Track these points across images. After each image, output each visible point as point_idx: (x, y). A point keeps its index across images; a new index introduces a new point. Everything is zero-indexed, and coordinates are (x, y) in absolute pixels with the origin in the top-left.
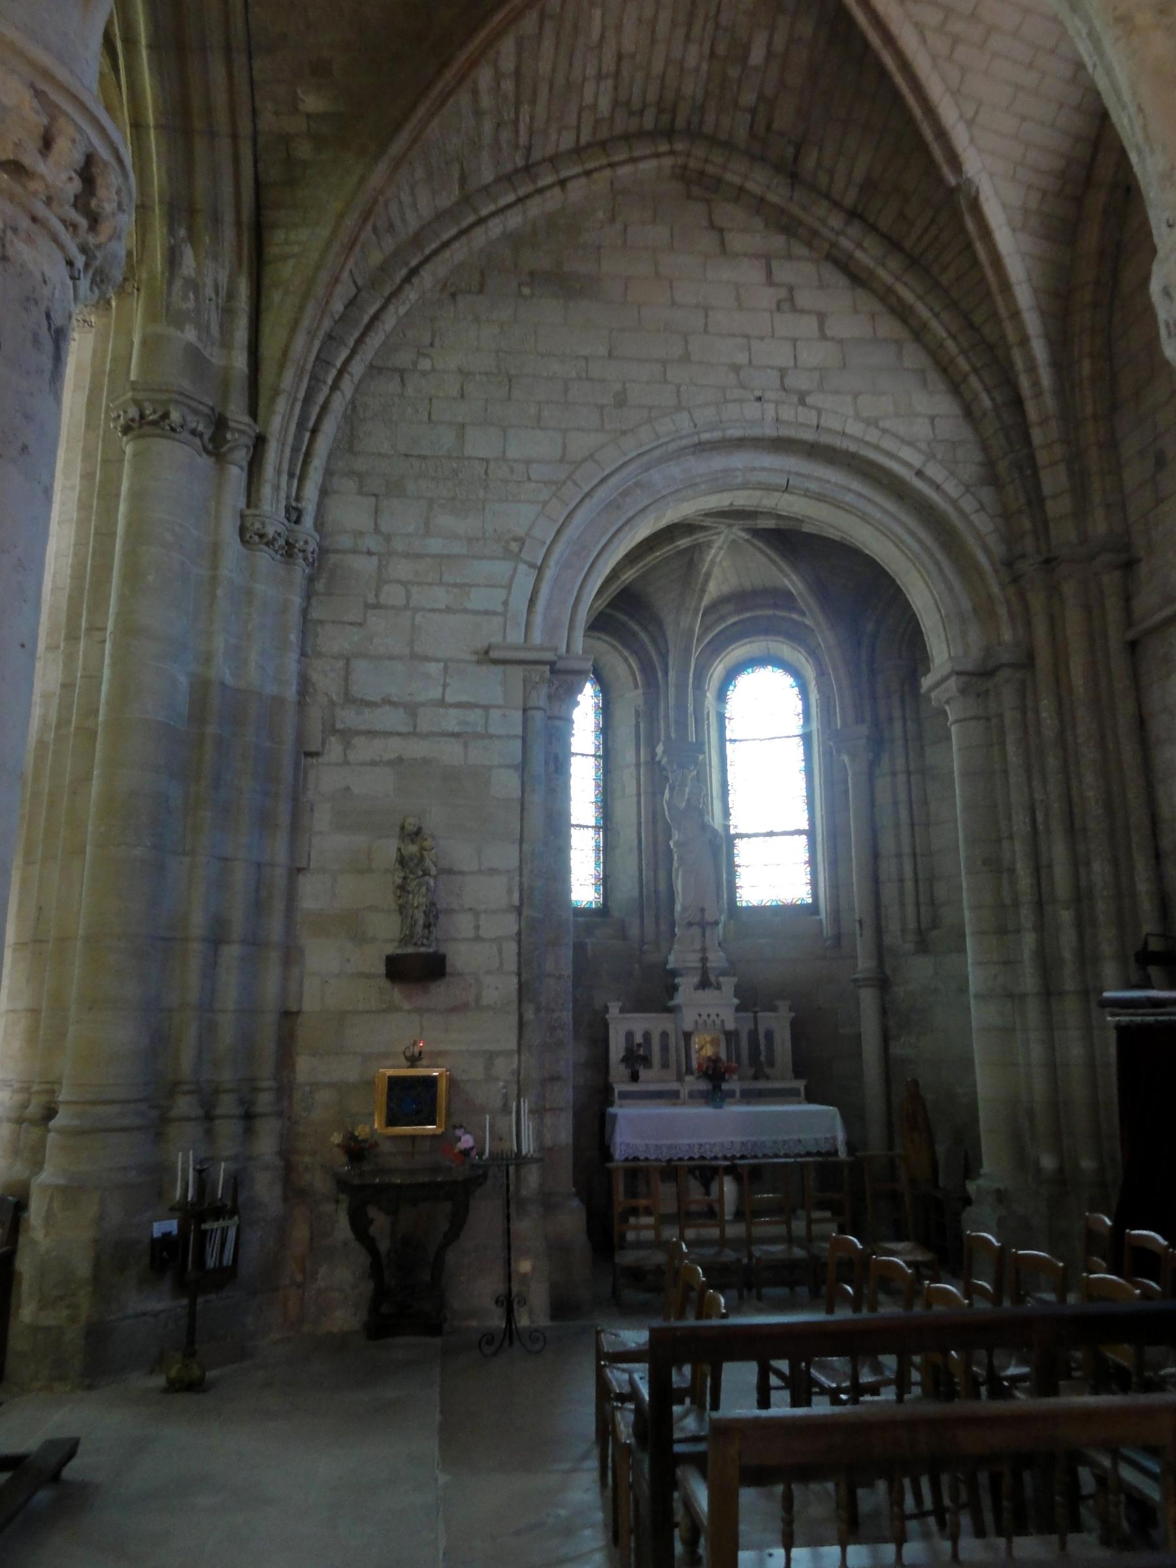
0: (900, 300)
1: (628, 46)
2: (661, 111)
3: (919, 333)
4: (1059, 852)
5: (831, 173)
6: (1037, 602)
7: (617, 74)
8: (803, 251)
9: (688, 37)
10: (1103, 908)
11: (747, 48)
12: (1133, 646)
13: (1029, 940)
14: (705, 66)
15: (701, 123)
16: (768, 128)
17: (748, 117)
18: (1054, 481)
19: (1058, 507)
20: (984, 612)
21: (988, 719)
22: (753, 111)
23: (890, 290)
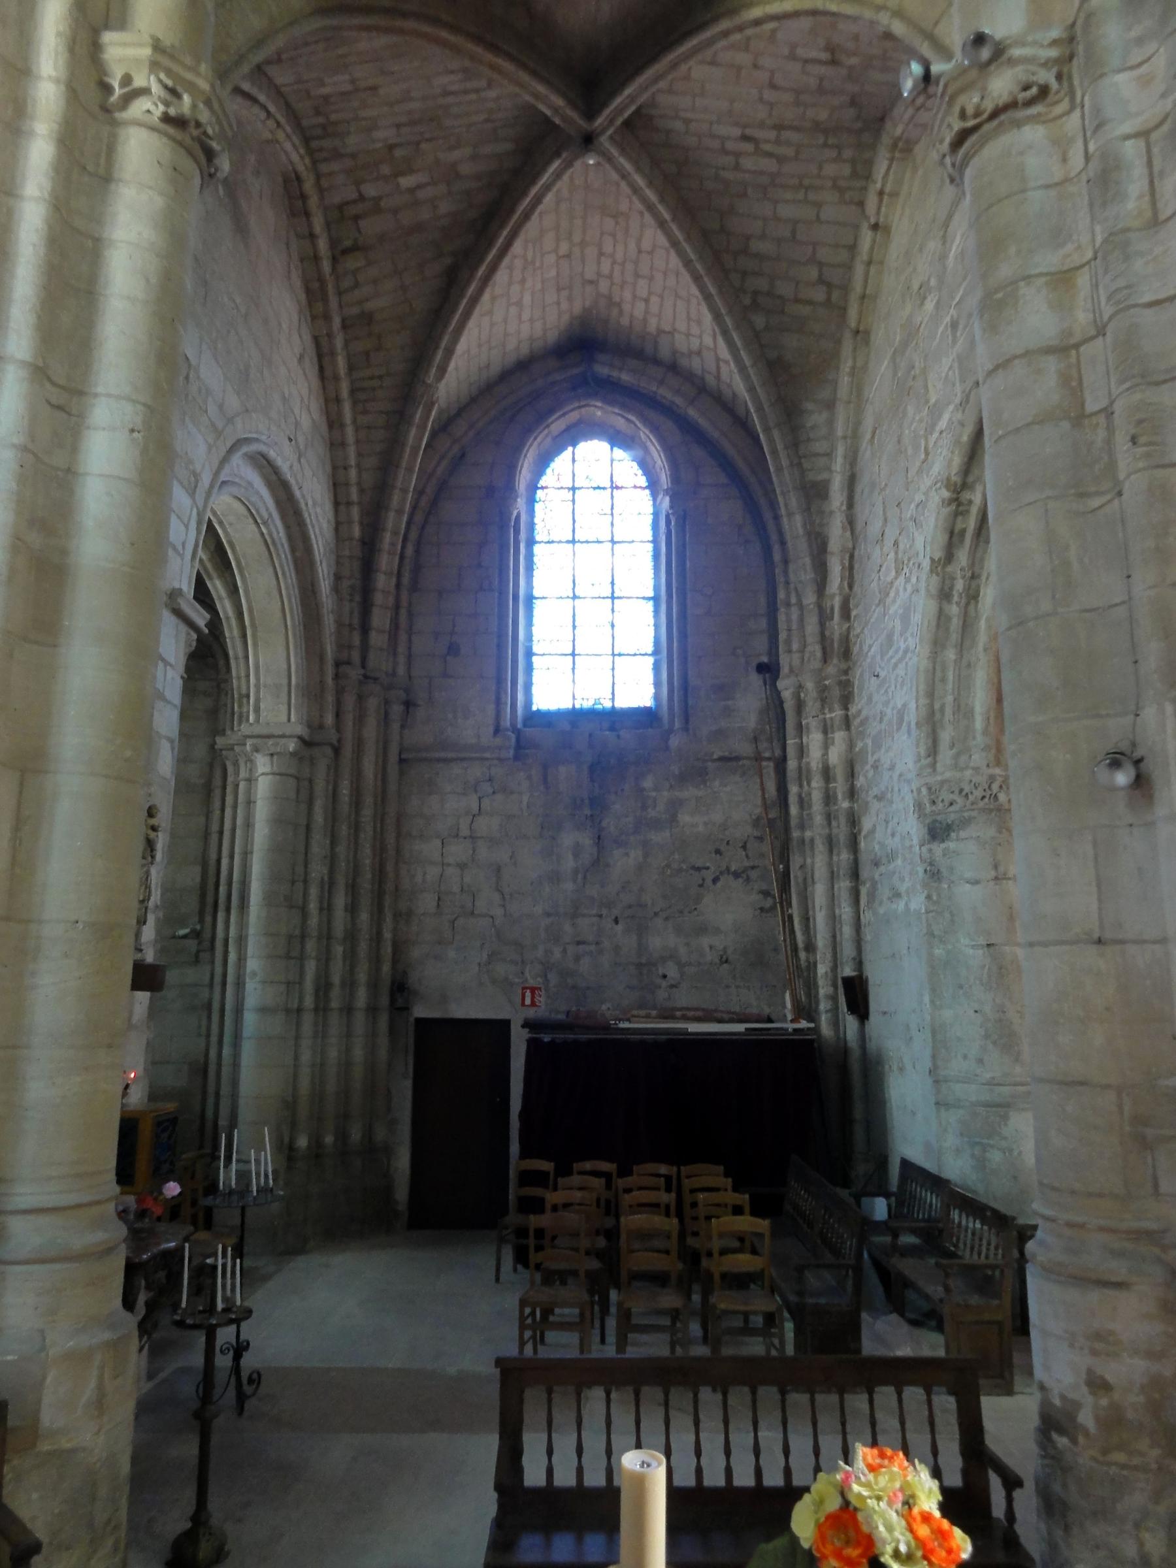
0: (340, 414)
1: (382, 92)
2: (324, 127)
3: (335, 445)
4: (340, 901)
5: (357, 285)
6: (350, 701)
7: (357, 90)
8: (309, 319)
9: (398, 126)
10: (363, 947)
11: (411, 171)
12: (402, 761)
13: (311, 967)
14: (379, 145)
15: (326, 160)
16: (356, 218)
17: (355, 195)
18: (380, 619)
19: (377, 639)
20: (313, 692)
21: (297, 778)
22: (362, 198)
23: (338, 400)
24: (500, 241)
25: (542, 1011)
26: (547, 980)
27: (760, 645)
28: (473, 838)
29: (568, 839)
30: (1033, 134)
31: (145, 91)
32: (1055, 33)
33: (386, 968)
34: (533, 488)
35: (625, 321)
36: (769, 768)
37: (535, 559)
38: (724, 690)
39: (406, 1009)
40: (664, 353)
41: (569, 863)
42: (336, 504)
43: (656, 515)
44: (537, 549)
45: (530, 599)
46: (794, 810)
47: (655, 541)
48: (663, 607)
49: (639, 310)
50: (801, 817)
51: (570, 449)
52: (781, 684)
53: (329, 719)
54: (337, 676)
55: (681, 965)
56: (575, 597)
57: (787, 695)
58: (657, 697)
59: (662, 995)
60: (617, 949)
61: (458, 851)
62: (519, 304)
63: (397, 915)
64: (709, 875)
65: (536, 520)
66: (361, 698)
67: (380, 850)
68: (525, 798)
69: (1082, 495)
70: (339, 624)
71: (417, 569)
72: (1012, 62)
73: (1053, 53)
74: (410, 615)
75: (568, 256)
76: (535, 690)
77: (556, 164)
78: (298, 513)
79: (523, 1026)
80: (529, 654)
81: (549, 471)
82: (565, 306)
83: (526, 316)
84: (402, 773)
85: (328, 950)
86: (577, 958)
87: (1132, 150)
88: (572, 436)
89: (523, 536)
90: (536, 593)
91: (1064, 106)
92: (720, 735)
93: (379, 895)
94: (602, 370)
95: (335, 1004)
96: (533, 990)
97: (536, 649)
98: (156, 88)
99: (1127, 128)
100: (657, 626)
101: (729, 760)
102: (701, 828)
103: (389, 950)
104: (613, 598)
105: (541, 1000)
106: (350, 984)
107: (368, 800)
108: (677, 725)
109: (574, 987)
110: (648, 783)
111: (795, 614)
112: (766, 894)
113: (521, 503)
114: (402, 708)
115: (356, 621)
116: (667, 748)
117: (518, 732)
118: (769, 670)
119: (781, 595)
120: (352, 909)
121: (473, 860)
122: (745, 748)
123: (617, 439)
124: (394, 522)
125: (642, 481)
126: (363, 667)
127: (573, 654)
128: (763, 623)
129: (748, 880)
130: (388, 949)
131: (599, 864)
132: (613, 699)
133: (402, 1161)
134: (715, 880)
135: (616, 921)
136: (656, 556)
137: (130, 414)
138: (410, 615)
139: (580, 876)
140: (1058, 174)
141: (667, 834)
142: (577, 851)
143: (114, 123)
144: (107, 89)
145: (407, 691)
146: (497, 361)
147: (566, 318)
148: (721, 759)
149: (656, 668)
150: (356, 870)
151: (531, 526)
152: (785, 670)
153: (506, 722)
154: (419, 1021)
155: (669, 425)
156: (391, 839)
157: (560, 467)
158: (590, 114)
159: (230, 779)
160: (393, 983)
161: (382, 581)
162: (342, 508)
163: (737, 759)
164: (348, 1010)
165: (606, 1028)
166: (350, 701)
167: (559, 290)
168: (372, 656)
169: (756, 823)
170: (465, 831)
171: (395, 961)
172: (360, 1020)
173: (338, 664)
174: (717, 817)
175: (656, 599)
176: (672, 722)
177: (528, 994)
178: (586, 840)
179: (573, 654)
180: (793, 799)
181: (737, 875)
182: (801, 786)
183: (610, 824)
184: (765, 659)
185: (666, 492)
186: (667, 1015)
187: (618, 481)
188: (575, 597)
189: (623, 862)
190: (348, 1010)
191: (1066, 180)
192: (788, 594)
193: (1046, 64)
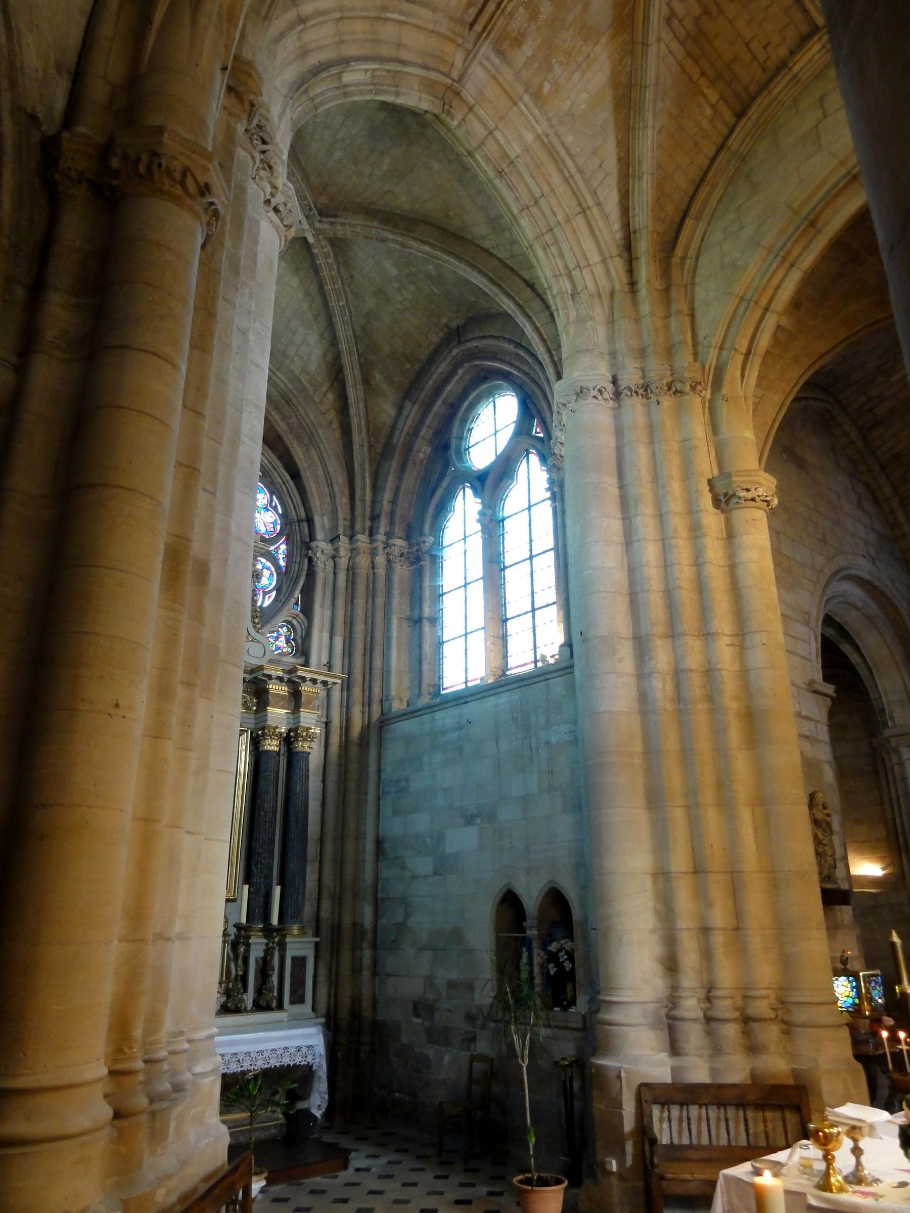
23: (892, 512)
78: (882, 594)
159: (888, 765)
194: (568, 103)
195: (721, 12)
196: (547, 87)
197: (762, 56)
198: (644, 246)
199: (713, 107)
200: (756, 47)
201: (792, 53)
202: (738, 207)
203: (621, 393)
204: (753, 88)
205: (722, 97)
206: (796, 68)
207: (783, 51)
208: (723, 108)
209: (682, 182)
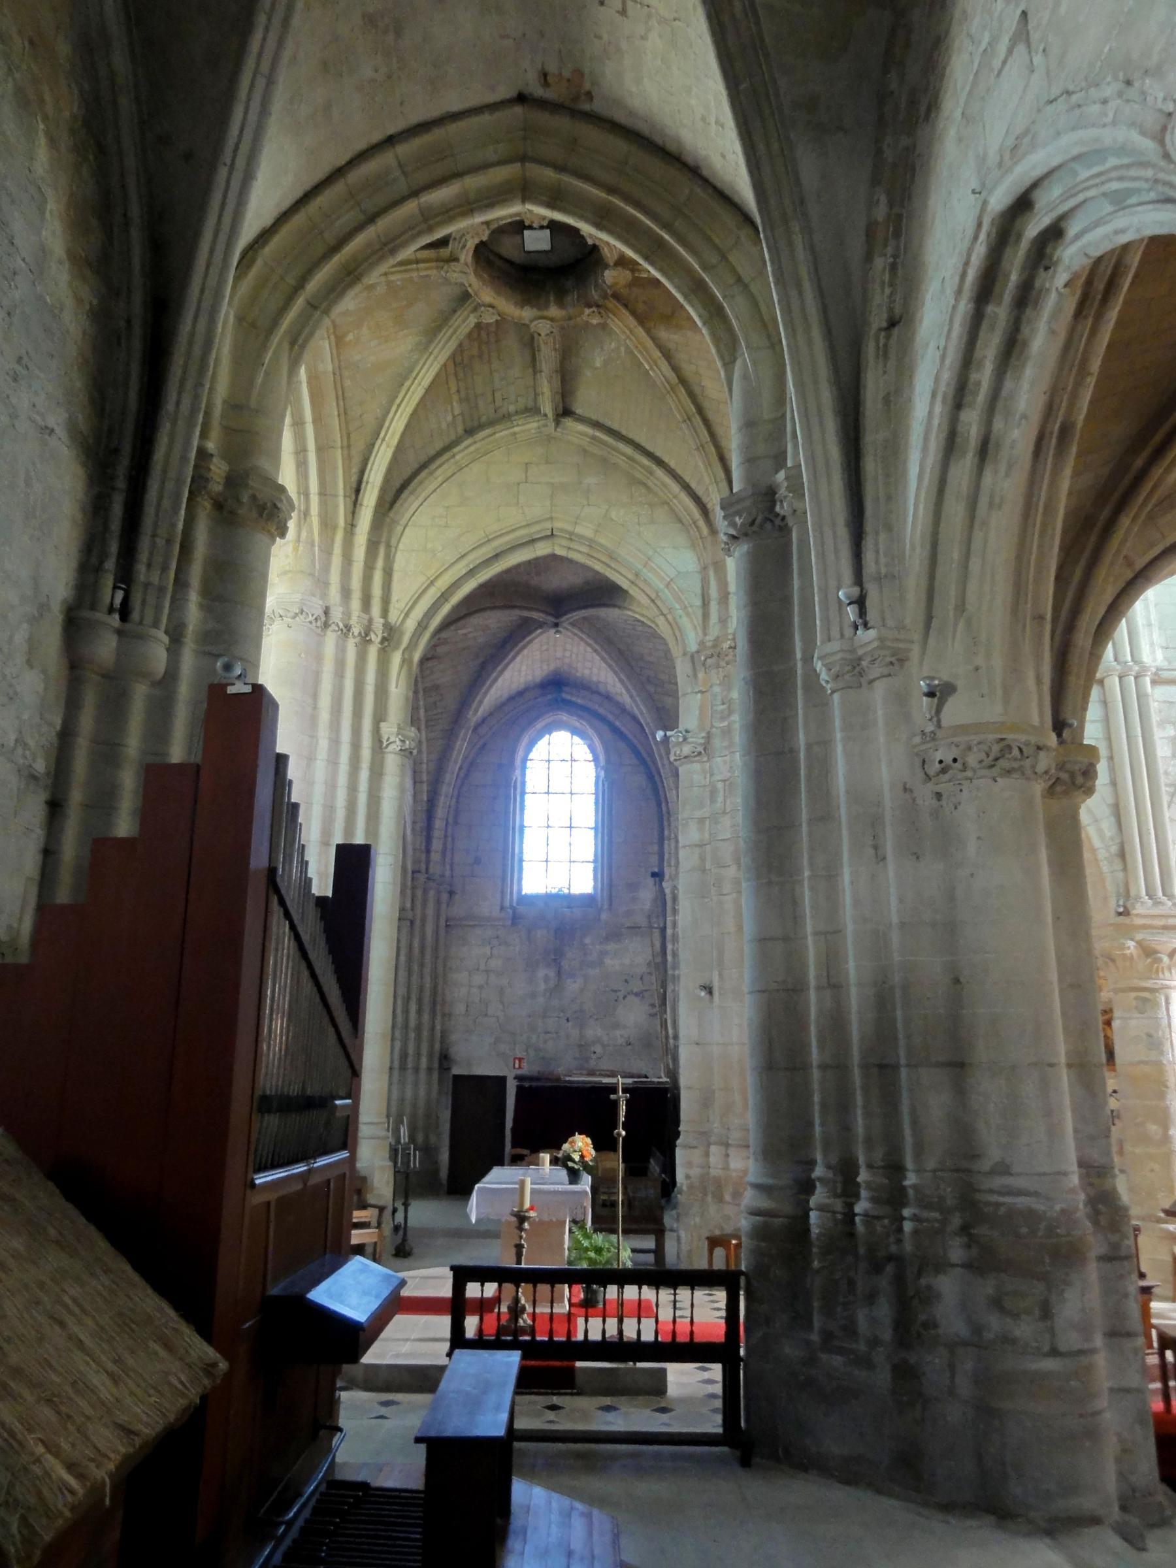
4: (413, 1007)
6: (419, 893)
10: (425, 1034)
12: (447, 926)
18: (436, 845)
19: (435, 857)
24: (510, 657)
25: (526, 1070)
26: (528, 1053)
27: (654, 859)
28: (487, 971)
29: (541, 973)
30: (697, 766)
31: (395, 742)
32: (703, 734)
33: (437, 1046)
34: (525, 760)
35: (578, 674)
36: (657, 934)
37: (526, 803)
38: (633, 887)
39: (449, 1069)
40: (602, 689)
41: (542, 987)
42: (415, 783)
43: (597, 777)
44: (527, 797)
45: (522, 827)
46: (669, 958)
47: (596, 794)
48: (600, 835)
49: (587, 672)
50: (674, 963)
51: (547, 736)
52: (664, 884)
53: (408, 905)
54: (413, 879)
55: (604, 1046)
56: (548, 827)
57: (667, 891)
58: (595, 887)
59: (592, 1064)
60: (568, 1036)
61: (478, 979)
62: (520, 671)
63: (444, 1015)
64: (621, 994)
65: (527, 779)
66: (425, 891)
67: (435, 977)
68: (517, 949)
69: (704, 897)
70: (414, 850)
71: (457, 811)
72: (689, 743)
73: (702, 741)
74: (453, 839)
75: (547, 650)
76: (524, 882)
77: (539, 631)
79: (515, 1078)
80: (521, 860)
81: (534, 749)
82: (545, 667)
83: (523, 673)
84: (447, 932)
85: (407, 1033)
86: (545, 1042)
87: (720, 785)
88: (549, 729)
89: (519, 791)
90: (526, 824)
91: (705, 759)
92: (629, 913)
93: (434, 1003)
94: (565, 696)
95: (410, 1065)
96: (520, 1060)
97: (524, 858)
98: (398, 743)
99: (719, 778)
100: (596, 845)
101: (634, 928)
102: (617, 968)
103: (439, 1035)
104: (571, 827)
105: (524, 1064)
106: (418, 1055)
107: (428, 951)
108: (606, 907)
109: (543, 1058)
110: (588, 940)
111: (673, 845)
112: (653, 1006)
113: (518, 772)
114: (448, 895)
115: (423, 848)
116: (599, 920)
117: (514, 909)
118: (658, 876)
119: (666, 833)
120: (419, 1012)
121: (487, 984)
122: (642, 921)
123: (575, 731)
124: (446, 790)
125: (590, 757)
126: (427, 872)
127: (547, 861)
128: (656, 848)
129: (643, 997)
130: (438, 1035)
131: (557, 989)
132: (569, 889)
133: (444, 1157)
134: (624, 997)
135: (568, 1020)
136: (596, 803)
137: (390, 859)
138: (453, 839)
139: (548, 994)
140: (703, 783)
141: (597, 971)
142: (546, 979)
143: (383, 753)
144: (381, 742)
145: (451, 885)
146: (506, 695)
147: (545, 673)
148: (628, 928)
149: (595, 870)
150: (421, 989)
151: (524, 783)
152: (667, 877)
153: (507, 904)
154: (456, 1077)
155: (605, 729)
156: (440, 970)
157: (541, 749)
158: (558, 616)
160: (441, 1054)
161: (438, 824)
162: (418, 784)
163: (639, 928)
164: (416, 1070)
165: (558, 1079)
166: (419, 893)
167: (542, 662)
168: (431, 865)
169: (649, 964)
170: (482, 967)
171: (442, 1042)
172: (423, 1075)
173: (413, 872)
174: (627, 961)
175: (596, 829)
176: (602, 905)
177: (517, 1062)
178: (552, 973)
179: (547, 861)
180: (669, 951)
181: (636, 995)
182: (674, 945)
183: (565, 964)
184: (656, 870)
185: (602, 768)
186: (592, 1073)
187: (575, 757)
188: (548, 827)
189: (573, 986)
190: (416, 1070)
191: (705, 786)
192: (670, 832)
193: (701, 744)
194: (358, 357)
195: (489, 362)
196: (350, 337)
197: (498, 403)
198: (370, 498)
199: (454, 417)
200: (498, 396)
201: (517, 413)
202: (448, 507)
203: (330, 626)
204: (484, 419)
205: (462, 414)
206: (516, 429)
207: (512, 408)
208: (459, 420)
209: (412, 461)
